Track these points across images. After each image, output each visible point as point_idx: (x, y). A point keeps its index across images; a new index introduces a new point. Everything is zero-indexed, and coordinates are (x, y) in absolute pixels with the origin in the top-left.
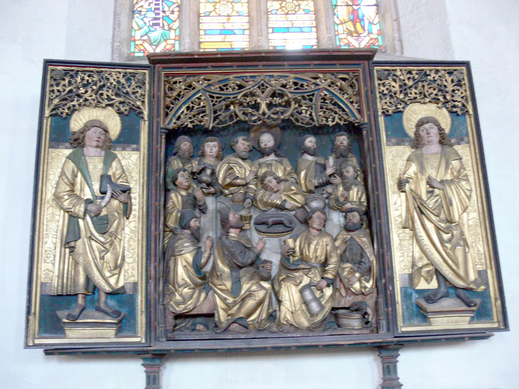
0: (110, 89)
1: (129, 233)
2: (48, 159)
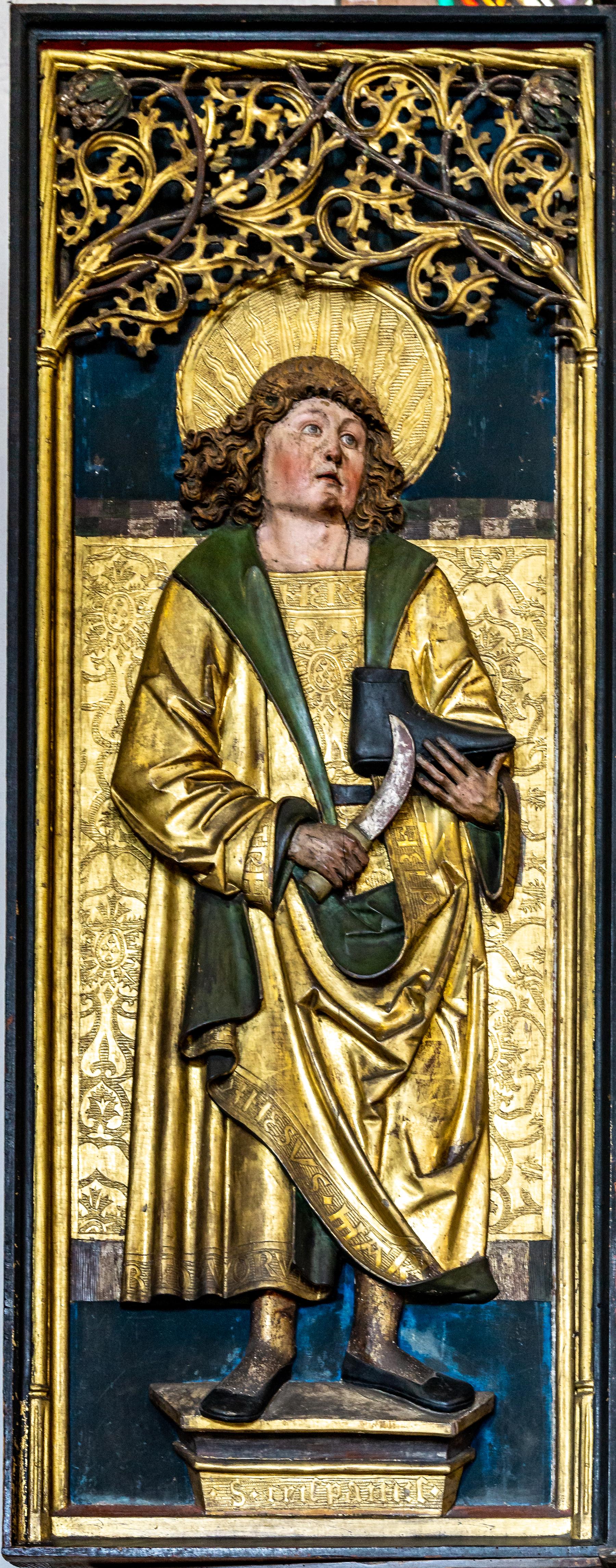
0: (384, 171)
1: (509, 987)
2: (72, 593)
